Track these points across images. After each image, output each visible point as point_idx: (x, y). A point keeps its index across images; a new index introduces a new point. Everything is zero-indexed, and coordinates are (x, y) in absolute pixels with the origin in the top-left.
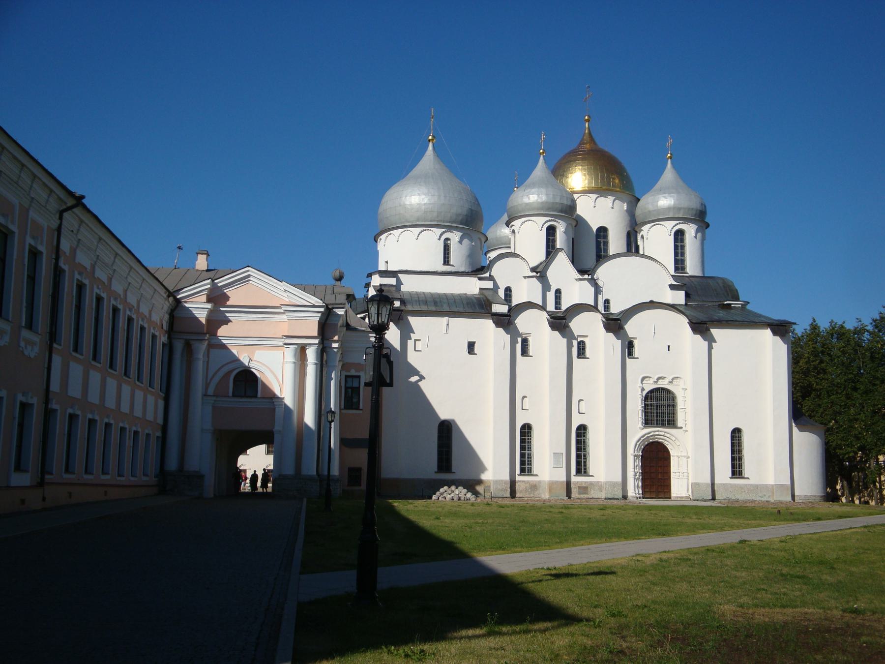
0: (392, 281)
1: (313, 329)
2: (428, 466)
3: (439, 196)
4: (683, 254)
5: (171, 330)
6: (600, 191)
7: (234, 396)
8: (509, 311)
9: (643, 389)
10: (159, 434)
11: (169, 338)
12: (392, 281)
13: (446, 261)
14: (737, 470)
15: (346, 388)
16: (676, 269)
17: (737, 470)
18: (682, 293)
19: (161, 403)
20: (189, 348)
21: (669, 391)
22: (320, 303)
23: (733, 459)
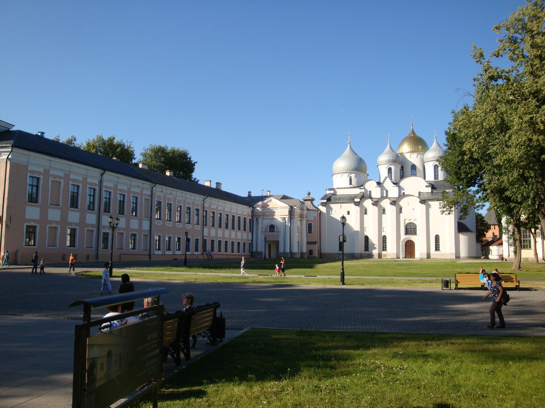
0: (332, 192)
1: (287, 213)
2: (335, 249)
3: (348, 163)
4: (438, 173)
5: (253, 216)
6: (412, 152)
7: (270, 232)
8: (360, 200)
9: (405, 223)
10: (250, 242)
11: (252, 217)
12: (332, 192)
13: (351, 184)
14: (437, 248)
15: (309, 227)
16: (435, 179)
17: (437, 248)
18: (430, 188)
19: (250, 235)
20: (257, 219)
21: (414, 224)
22: (288, 206)
23: (436, 245)
